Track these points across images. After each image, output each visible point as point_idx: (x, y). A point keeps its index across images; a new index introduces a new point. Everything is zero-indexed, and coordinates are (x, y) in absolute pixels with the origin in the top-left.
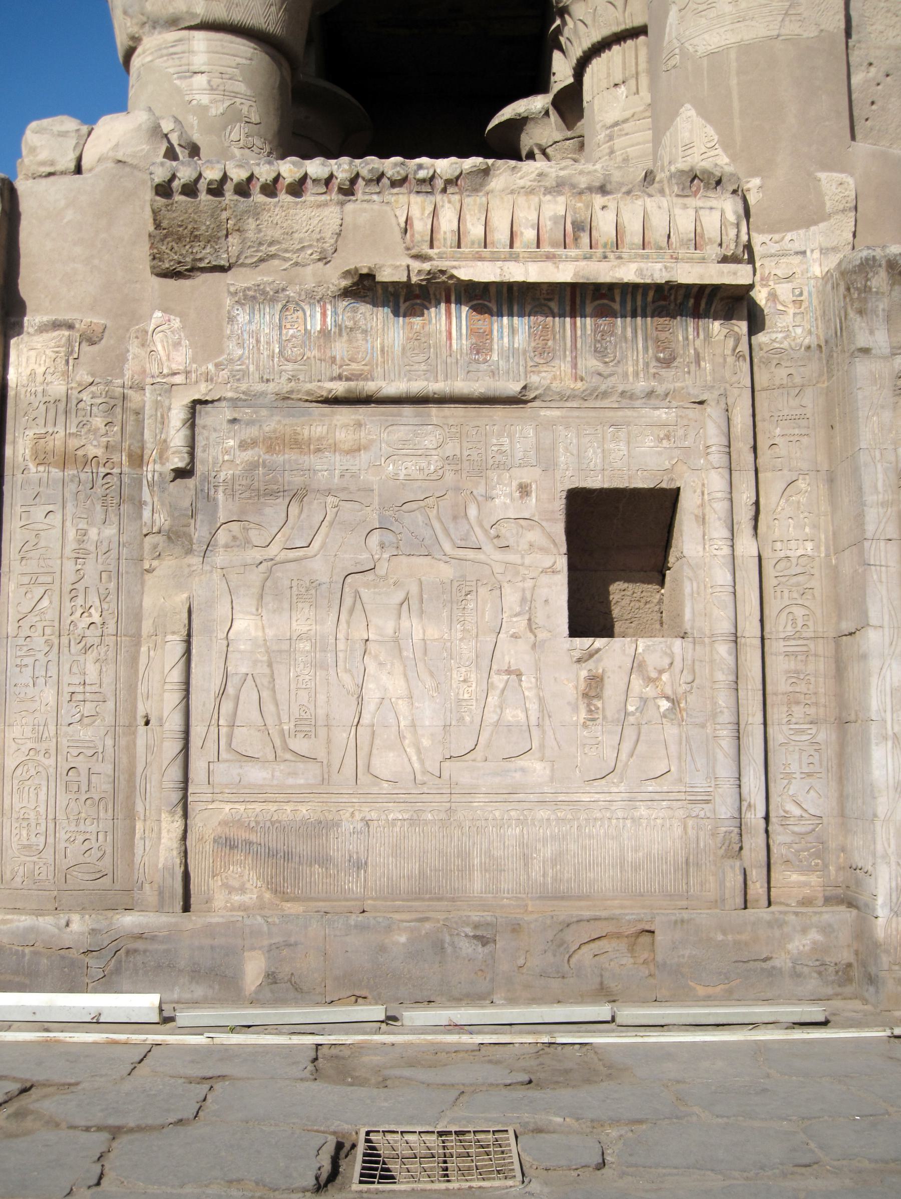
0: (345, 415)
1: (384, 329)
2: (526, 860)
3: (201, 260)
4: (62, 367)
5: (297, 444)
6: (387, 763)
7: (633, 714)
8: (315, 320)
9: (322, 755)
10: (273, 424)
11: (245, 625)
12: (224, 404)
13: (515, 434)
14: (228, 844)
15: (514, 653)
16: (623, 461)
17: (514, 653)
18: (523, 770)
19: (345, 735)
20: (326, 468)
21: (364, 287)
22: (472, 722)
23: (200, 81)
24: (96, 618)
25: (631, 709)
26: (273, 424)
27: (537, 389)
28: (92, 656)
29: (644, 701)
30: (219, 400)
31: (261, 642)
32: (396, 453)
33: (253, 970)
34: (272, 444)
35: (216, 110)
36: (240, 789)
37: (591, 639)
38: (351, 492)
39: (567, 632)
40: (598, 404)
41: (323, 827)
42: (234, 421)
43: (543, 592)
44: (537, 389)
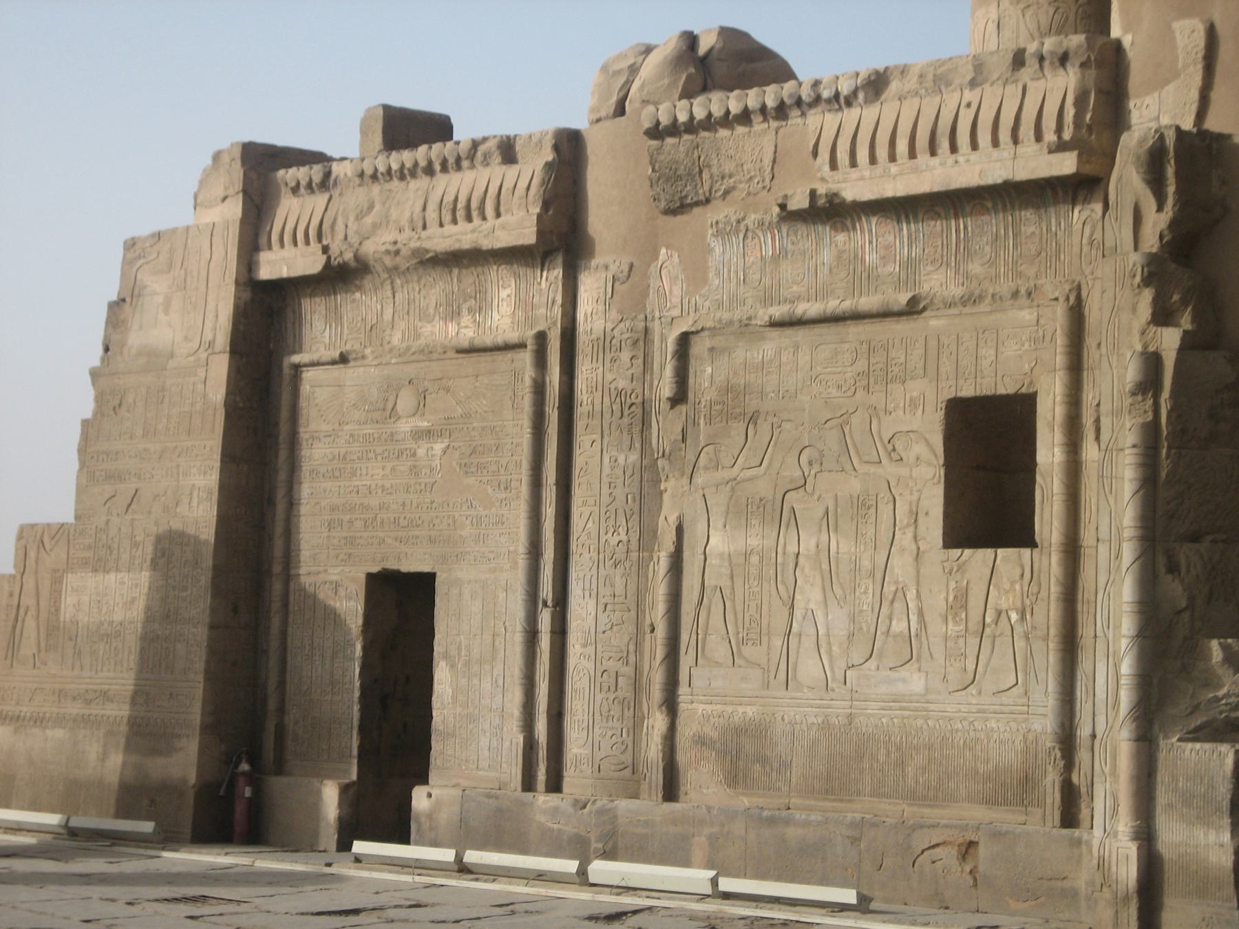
2: (901, 764)
3: (686, 197)
4: (601, 307)
7: (989, 626)
9: (764, 661)
12: (706, 333)
14: (701, 741)
18: (904, 680)
19: (780, 643)
22: (869, 630)
24: (624, 537)
25: (988, 620)
27: (925, 298)
28: (620, 570)
29: (999, 613)
30: (702, 329)
31: (726, 556)
37: (959, 551)
39: (940, 541)
40: (975, 309)
42: (712, 349)
43: (925, 504)
44: (925, 298)
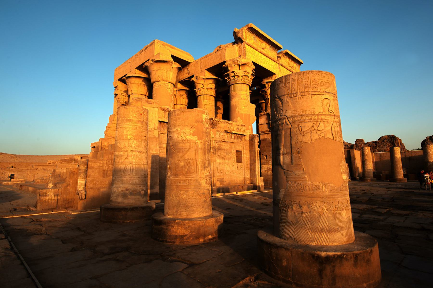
0: (224, 143)
1: (226, 135)
5: (221, 145)
6: (227, 173)
8: (222, 134)
10: (219, 143)
11: (218, 161)
13: (233, 145)
15: (234, 164)
16: (239, 148)
17: (234, 164)
20: (223, 147)
21: (226, 132)
23: (169, 90)
26: (219, 143)
32: (226, 146)
33: (221, 191)
34: (219, 145)
35: (171, 94)
36: (218, 176)
38: (224, 150)
41: (223, 178)
